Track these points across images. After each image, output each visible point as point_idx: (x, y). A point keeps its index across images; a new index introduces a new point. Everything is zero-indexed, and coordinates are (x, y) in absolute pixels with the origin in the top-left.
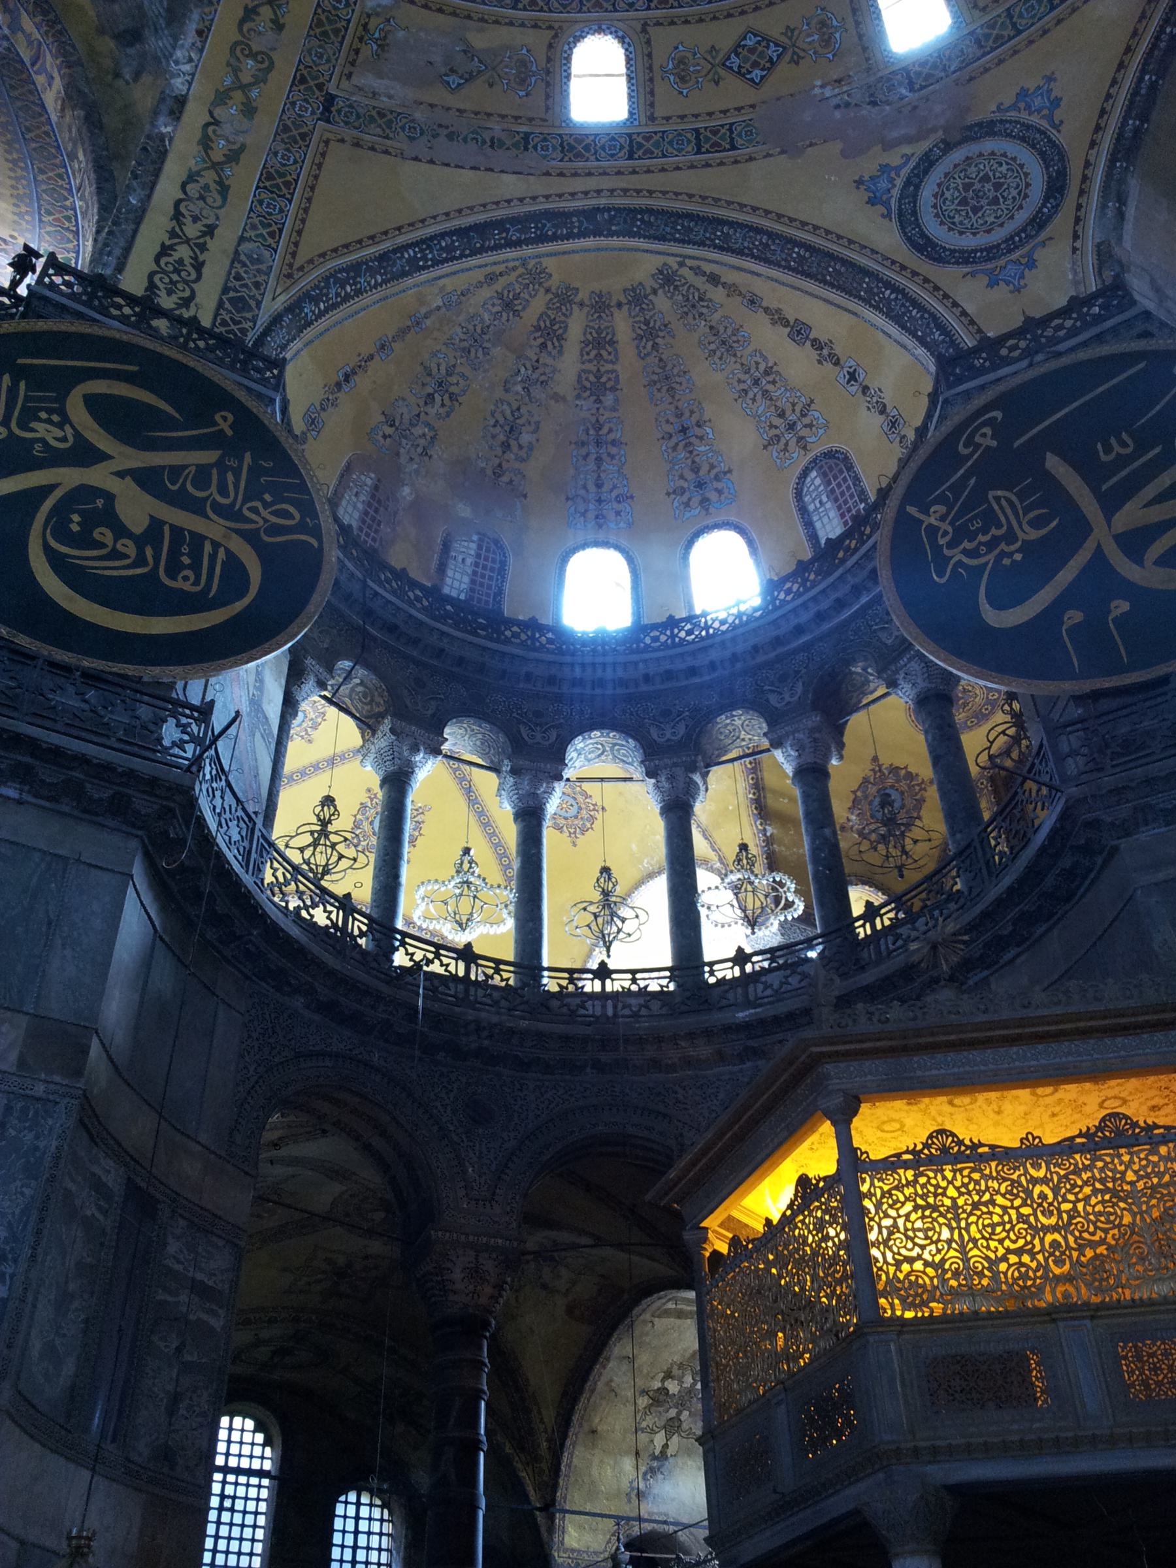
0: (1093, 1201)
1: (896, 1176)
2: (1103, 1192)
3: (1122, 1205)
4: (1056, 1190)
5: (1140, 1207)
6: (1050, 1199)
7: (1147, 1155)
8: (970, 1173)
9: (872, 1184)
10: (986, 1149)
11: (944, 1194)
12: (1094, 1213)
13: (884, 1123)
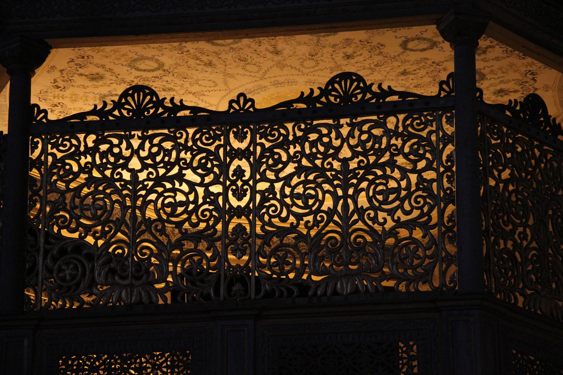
0: (295, 180)
1: (74, 142)
2: (308, 171)
3: (326, 187)
4: (255, 168)
5: (345, 191)
6: (247, 175)
7: (371, 128)
8: (162, 141)
9: (44, 151)
10: (187, 113)
11: (125, 166)
12: (293, 196)
13: (135, 60)
